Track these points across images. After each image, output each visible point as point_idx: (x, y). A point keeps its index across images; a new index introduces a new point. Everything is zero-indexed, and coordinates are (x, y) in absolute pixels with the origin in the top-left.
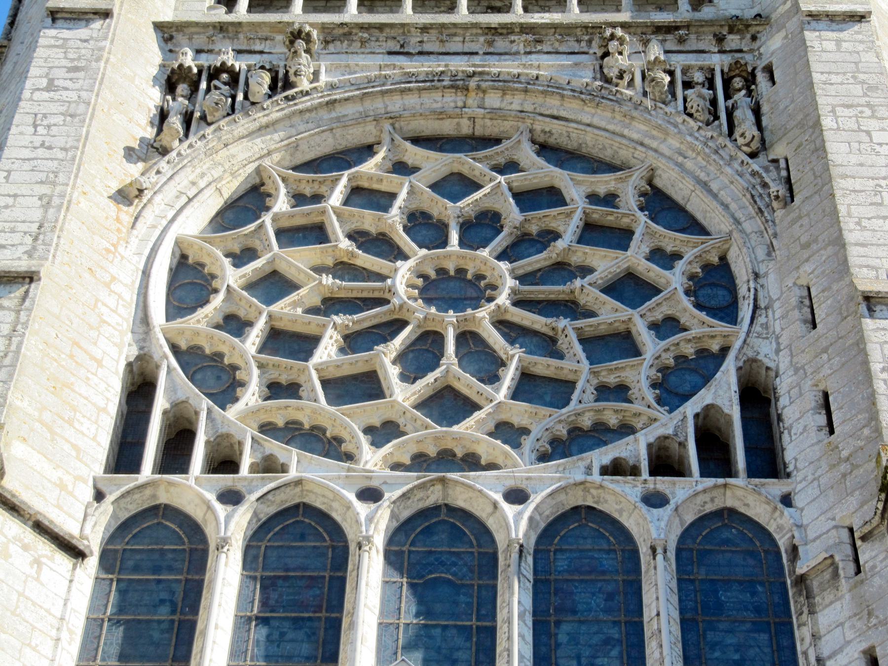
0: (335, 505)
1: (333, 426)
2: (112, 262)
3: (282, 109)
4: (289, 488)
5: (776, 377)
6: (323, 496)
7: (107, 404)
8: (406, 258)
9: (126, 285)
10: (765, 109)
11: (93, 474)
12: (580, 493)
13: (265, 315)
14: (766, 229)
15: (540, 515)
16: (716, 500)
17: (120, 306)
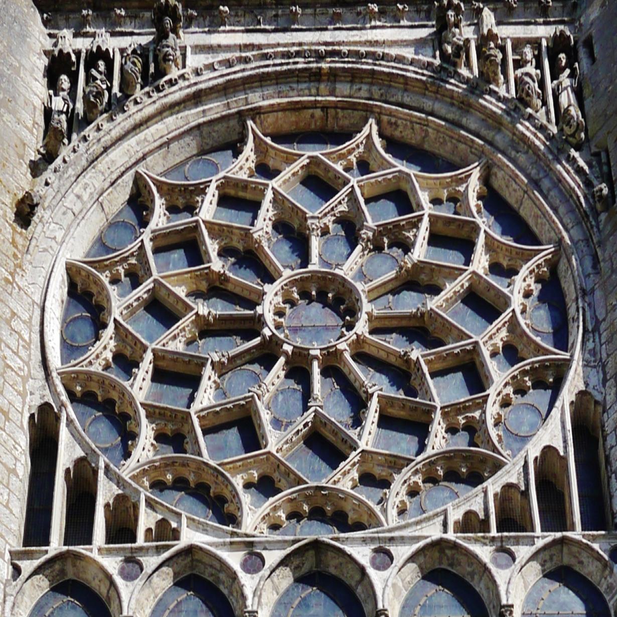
0: (222, 576)
1: (216, 483)
2: (10, 294)
3: (154, 102)
4: (181, 558)
5: (604, 412)
6: (211, 566)
7: (15, 465)
8: (271, 280)
9: (24, 322)
10: (586, 92)
11: (8, 547)
12: (437, 554)
13: (149, 356)
14: (591, 236)
15: (403, 581)
16: (555, 558)
17: (21, 347)
